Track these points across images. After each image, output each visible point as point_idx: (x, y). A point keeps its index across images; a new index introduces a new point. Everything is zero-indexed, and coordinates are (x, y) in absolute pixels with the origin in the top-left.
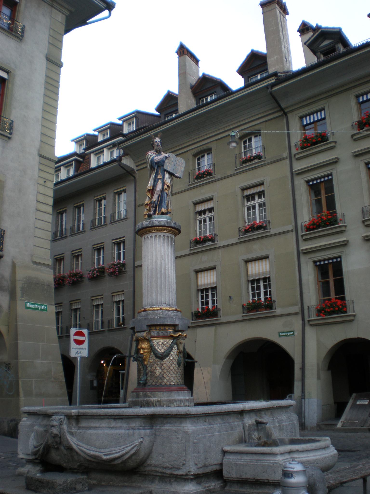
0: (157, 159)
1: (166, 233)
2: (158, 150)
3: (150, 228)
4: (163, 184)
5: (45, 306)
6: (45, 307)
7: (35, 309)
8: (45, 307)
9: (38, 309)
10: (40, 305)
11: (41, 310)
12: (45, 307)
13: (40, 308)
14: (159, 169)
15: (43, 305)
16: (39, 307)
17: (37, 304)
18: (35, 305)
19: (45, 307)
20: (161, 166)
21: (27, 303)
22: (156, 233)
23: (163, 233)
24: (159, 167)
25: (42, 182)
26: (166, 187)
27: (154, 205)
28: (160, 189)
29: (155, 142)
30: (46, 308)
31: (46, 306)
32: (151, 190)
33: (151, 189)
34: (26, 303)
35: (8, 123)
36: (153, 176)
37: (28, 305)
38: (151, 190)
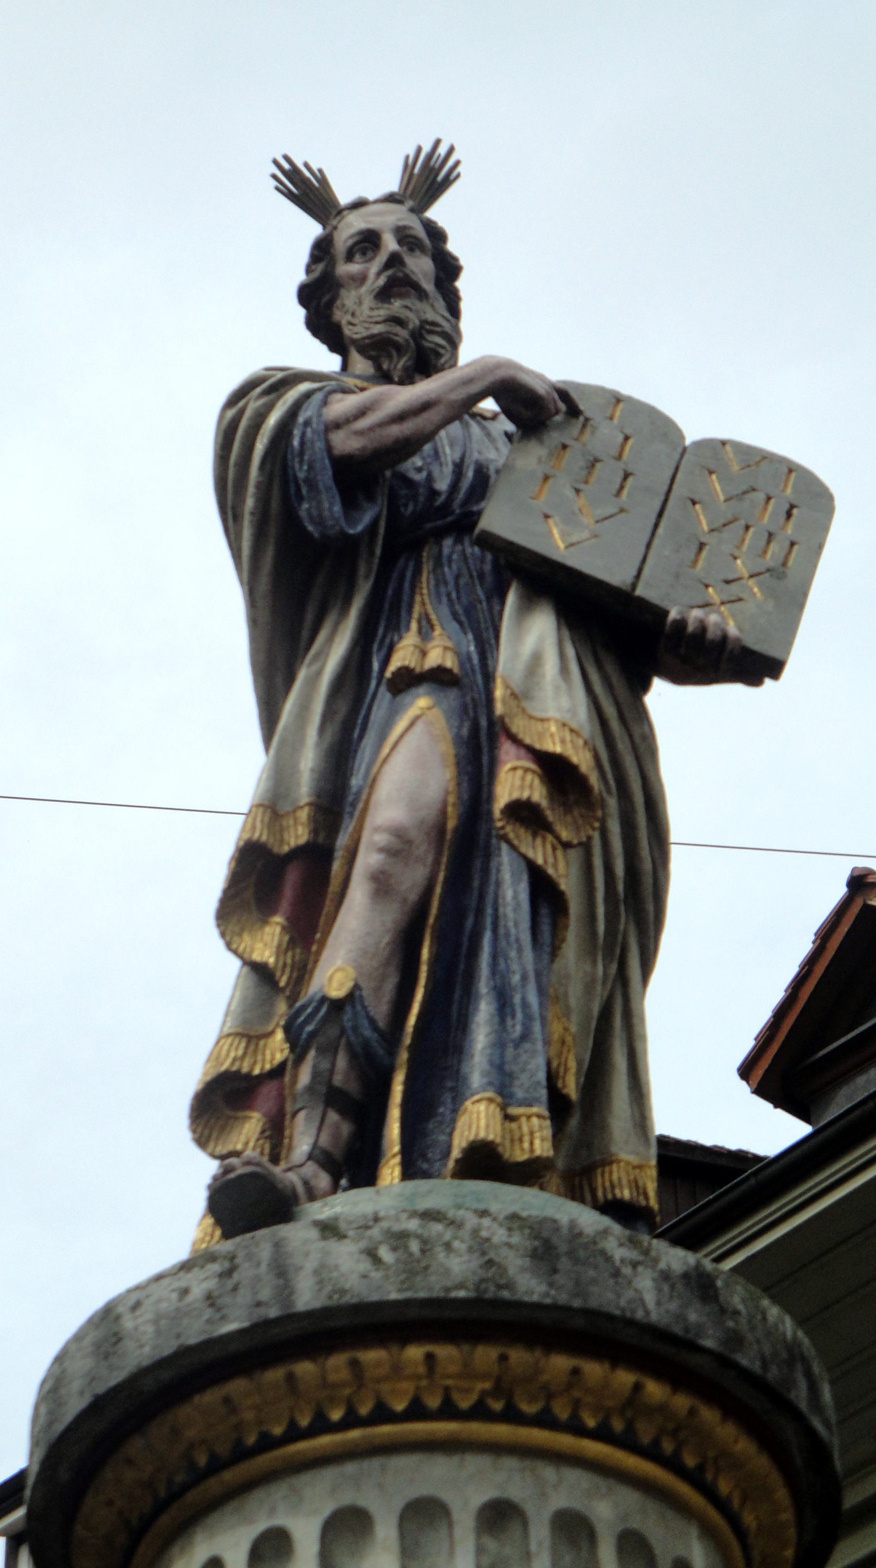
0: (362, 412)
1: (549, 1472)
2: (402, 334)
3: (237, 1386)
14: (418, 572)
20: (439, 535)
22: (350, 1468)
23: (474, 1462)
24: (415, 548)
27: (342, 1062)
28: (430, 814)
29: (350, 257)
32: (292, 877)
33: (298, 852)
36: (319, 673)
38: (292, 877)
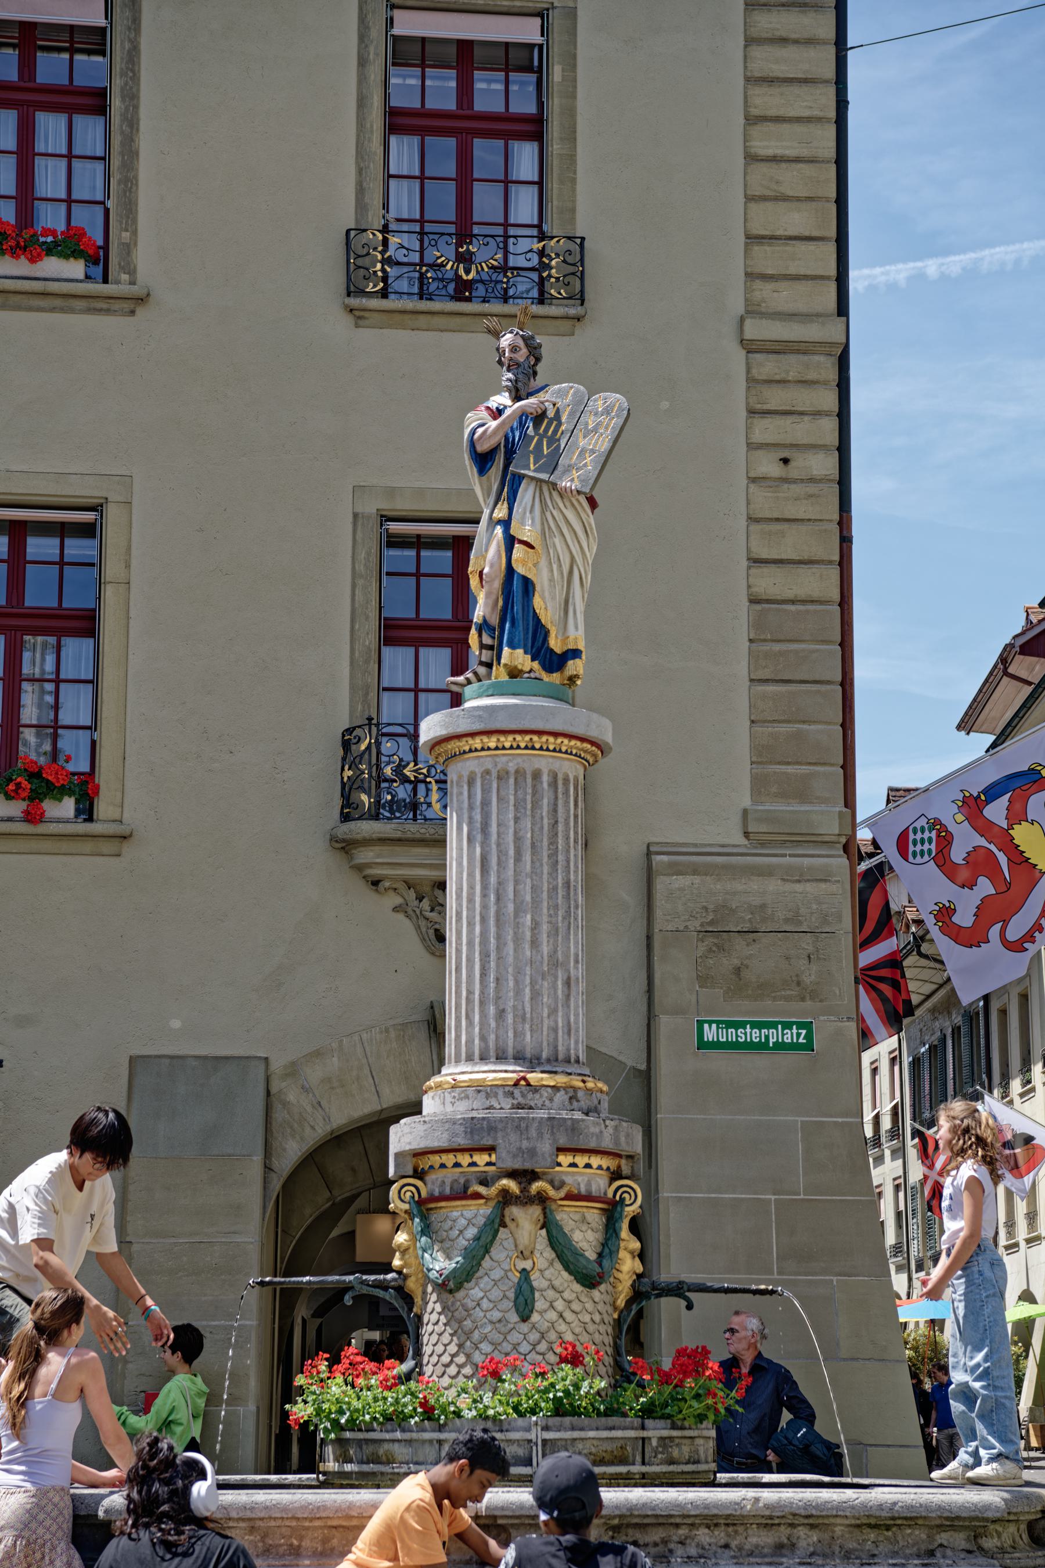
4: (510, 541)
5: (801, 1025)
6: (799, 1035)
7: (749, 1046)
8: (804, 1032)
9: (762, 1046)
10: (773, 1025)
11: (780, 1046)
12: (804, 1032)
13: (771, 1041)
15: (787, 1025)
16: (767, 1037)
17: (756, 1025)
18: (748, 1030)
19: (799, 1035)
21: (706, 1026)
25: (775, 469)
26: (518, 550)
30: (809, 1037)
31: (808, 1026)
34: (700, 1023)
35: (557, 255)
37: (710, 1033)
